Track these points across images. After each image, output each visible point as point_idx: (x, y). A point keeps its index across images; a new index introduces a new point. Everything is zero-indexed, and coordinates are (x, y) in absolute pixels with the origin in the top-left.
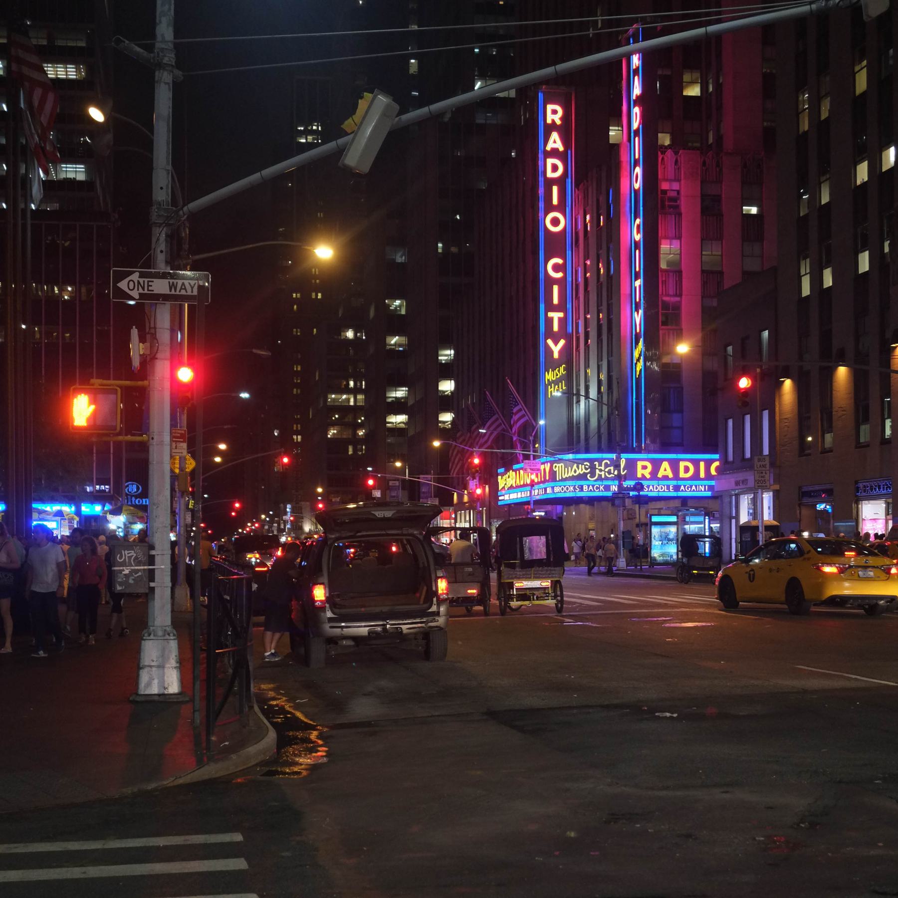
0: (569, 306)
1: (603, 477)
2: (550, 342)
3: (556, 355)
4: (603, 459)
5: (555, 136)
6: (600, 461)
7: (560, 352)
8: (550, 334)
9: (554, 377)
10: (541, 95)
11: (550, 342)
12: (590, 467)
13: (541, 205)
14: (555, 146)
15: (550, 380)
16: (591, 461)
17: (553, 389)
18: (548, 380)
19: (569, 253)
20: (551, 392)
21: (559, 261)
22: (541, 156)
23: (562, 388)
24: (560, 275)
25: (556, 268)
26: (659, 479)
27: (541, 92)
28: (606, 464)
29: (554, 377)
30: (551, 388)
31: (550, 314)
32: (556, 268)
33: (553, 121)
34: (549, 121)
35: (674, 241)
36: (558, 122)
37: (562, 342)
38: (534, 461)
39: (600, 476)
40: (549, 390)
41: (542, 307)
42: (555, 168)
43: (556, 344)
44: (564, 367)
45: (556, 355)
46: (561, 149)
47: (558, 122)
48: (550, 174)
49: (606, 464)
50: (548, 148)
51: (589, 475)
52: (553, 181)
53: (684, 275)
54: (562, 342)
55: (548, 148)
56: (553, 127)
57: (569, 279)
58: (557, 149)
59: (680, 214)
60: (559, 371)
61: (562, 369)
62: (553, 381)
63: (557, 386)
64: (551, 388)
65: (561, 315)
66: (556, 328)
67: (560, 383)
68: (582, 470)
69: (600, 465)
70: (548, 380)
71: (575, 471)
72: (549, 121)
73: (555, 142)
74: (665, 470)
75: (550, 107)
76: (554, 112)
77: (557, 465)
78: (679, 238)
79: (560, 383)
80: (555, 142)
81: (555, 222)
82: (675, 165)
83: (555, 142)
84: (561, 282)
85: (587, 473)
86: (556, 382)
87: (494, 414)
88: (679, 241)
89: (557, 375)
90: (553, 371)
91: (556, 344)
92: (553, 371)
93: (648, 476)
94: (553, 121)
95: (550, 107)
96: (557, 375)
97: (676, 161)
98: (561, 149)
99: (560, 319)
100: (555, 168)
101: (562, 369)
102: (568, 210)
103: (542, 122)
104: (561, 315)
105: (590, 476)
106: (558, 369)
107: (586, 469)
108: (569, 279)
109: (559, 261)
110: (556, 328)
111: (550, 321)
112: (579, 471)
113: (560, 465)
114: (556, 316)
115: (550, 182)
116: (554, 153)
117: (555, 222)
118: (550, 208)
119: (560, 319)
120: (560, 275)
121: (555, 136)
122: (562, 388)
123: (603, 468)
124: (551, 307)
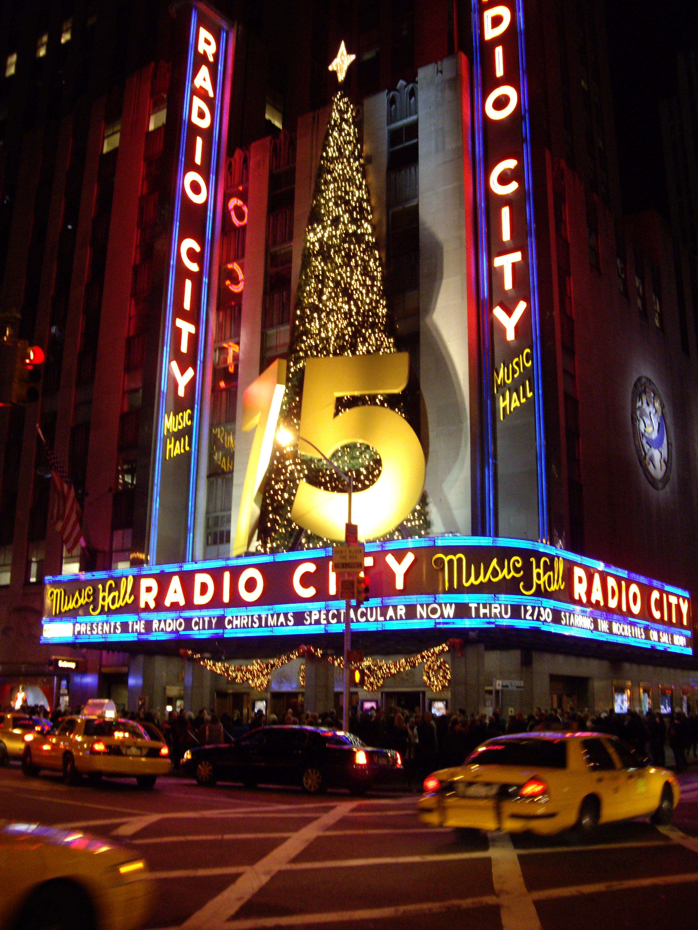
5: (204, 71)
7: (186, 387)
9: (175, 427)
15: (171, 431)
16: (525, 554)
17: (172, 446)
18: (168, 430)
20: (170, 450)
23: (184, 448)
24: (194, 267)
25: (191, 253)
29: (175, 427)
30: (170, 443)
31: (180, 323)
34: (201, 50)
36: (211, 59)
40: (168, 447)
43: (183, 371)
44: (189, 414)
51: (522, 584)
54: (190, 373)
60: (182, 418)
63: (178, 442)
64: (170, 443)
67: (182, 439)
68: (509, 572)
70: (168, 430)
71: (495, 573)
76: (208, 42)
79: (182, 439)
84: (196, 278)
86: (178, 436)
89: (179, 424)
91: (183, 371)
95: (204, 34)
96: (179, 424)
99: (190, 334)
100: (201, 115)
102: (212, 177)
104: (192, 329)
105: (524, 587)
106: (181, 414)
107: (517, 570)
111: (177, 332)
112: (504, 574)
117: (196, 188)
119: (190, 334)
120: (194, 267)
121: (204, 71)
122: (184, 448)
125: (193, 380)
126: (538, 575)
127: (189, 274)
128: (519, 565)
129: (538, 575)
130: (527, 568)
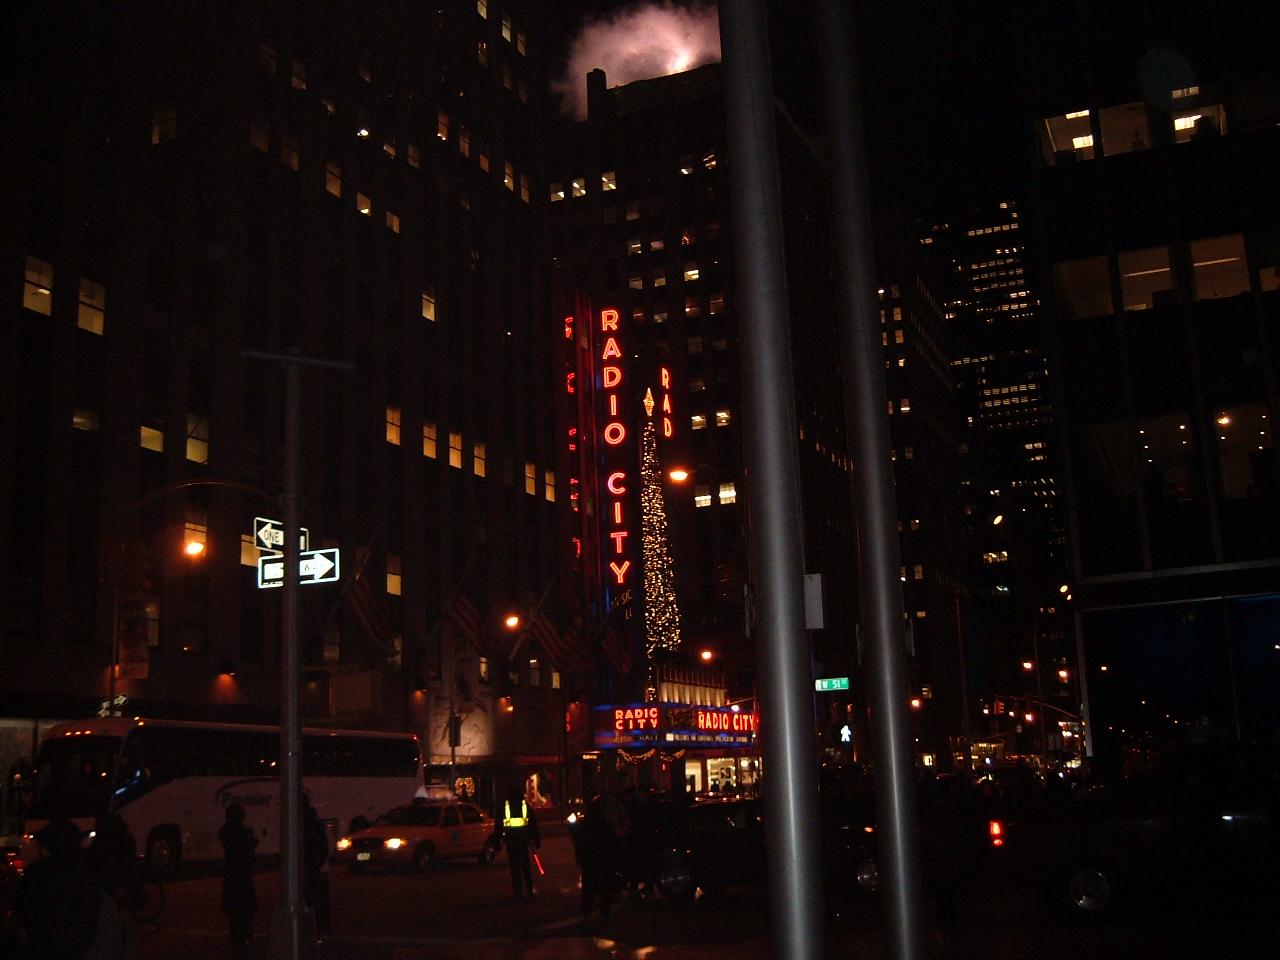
3: (620, 580)
5: (611, 342)
7: (626, 576)
14: (611, 353)
21: (621, 475)
25: (617, 483)
31: (613, 535)
32: (617, 483)
36: (614, 327)
37: (627, 564)
42: (612, 376)
43: (620, 567)
45: (620, 580)
46: (619, 355)
47: (614, 327)
48: (607, 383)
50: (605, 357)
52: (612, 390)
54: (627, 564)
56: (610, 333)
60: (625, 597)
65: (625, 534)
81: (615, 433)
83: (612, 349)
91: (620, 567)
99: (623, 538)
100: (612, 376)
104: (625, 534)
109: (621, 475)
116: (612, 361)
119: (623, 538)
121: (611, 342)
127: (617, 498)
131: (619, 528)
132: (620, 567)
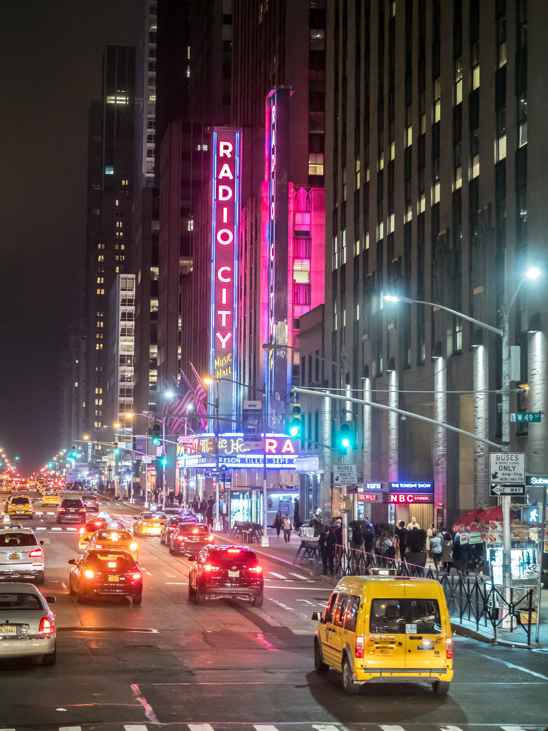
0: (235, 305)
1: (237, 451)
2: (218, 335)
3: (224, 346)
4: (238, 437)
5: (226, 167)
6: (235, 438)
8: (218, 328)
10: (215, 135)
11: (218, 335)
12: (227, 444)
13: (214, 224)
14: (226, 175)
19: (236, 263)
21: (229, 269)
22: (214, 182)
23: (228, 373)
25: (225, 274)
26: (283, 454)
27: (215, 131)
28: (240, 441)
30: (219, 372)
31: (220, 312)
32: (225, 274)
33: (225, 154)
34: (221, 155)
35: (305, 260)
36: (229, 156)
38: (188, 437)
39: (235, 451)
41: (213, 307)
45: (224, 346)
46: (231, 177)
47: (229, 156)
49: (240, 441)
50: (220, 177)
53: (312, 287)
54: (229, 335)
55: (220, 177)
57: (236, 283)
58: (228, 177)
59: (310, 239)
61: (228, 357)
62: (221, 367)
65: (229, 313)
66: (224, 324)
69: (235, 442)
70: (217, 366)
72: (221, 155)
73: (226, 172)
74: (288, 447)
75: (222, 144)
77: (203, 441)
78: (310, 258)
80: (226, 172)
81: (225, 237)
82: (307, 199)
84: (229, 286)
85: (224, 449)
87: (188, 390)
88: (309, 261)
90: (221, 359)
92: (221, 359)
93: (274, 451)
94: (225, 154)
95: (222, 144)
96: (224, 362)
97: (308, 196)
98: (231, 177)
100: (225, 193)
101: (228, 357)
103: (216, 156)
104: (229, 313)
107: (224, 445)
108: (236, 283)
109: (229, 269)
110: (224, 324)
111: (218, 318)
113: (205, 441)
114: (224, 313)
115: (221, 205)
116: (225, 181)
117: (225, 237)
118: (221, 225)
120: (228, 280)
121: (226, 167)
123: (237, 444)
124: (220, 306)
125: (231, 338)
126: (235, 446)
128: (225, 443)
129: (235, 446)
130: (229, 444)
131: (224, 308)
132: (224, 338)
